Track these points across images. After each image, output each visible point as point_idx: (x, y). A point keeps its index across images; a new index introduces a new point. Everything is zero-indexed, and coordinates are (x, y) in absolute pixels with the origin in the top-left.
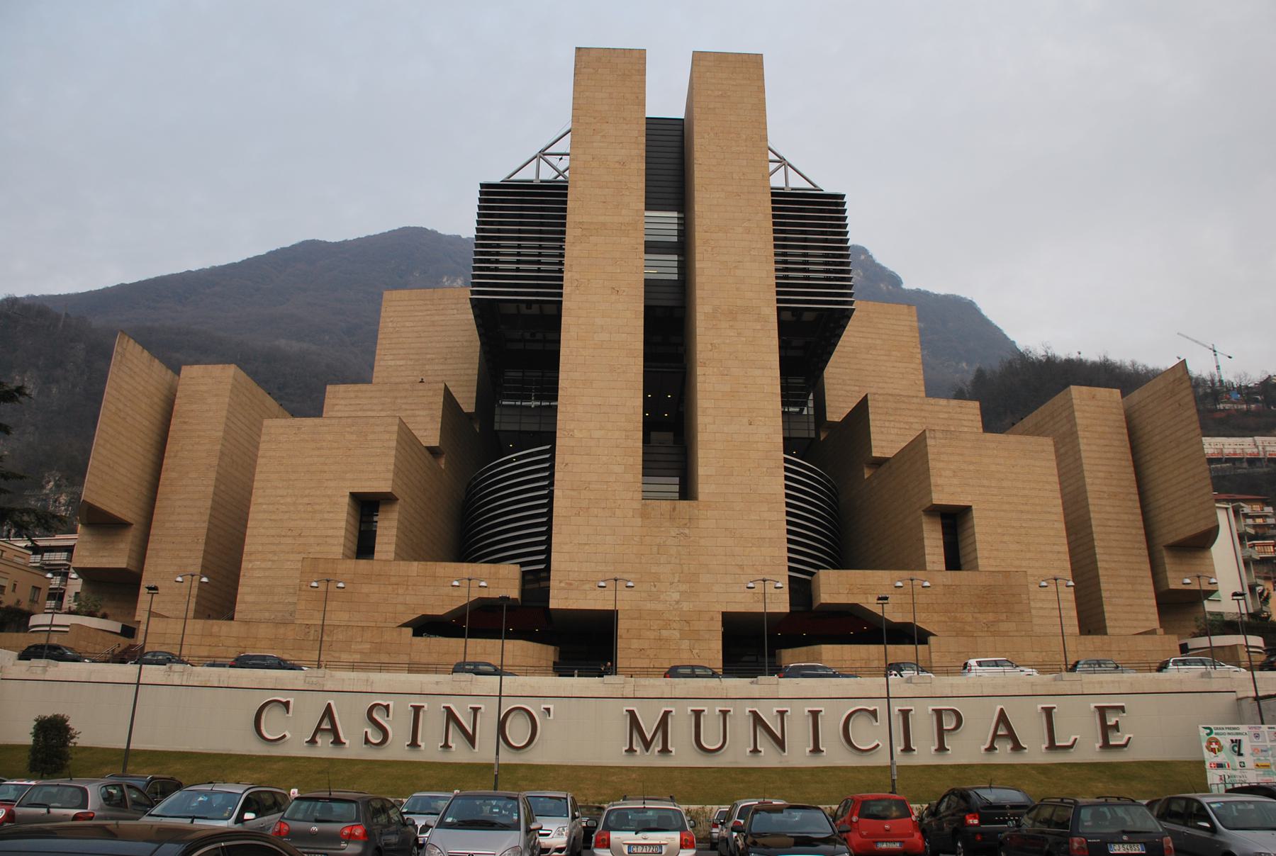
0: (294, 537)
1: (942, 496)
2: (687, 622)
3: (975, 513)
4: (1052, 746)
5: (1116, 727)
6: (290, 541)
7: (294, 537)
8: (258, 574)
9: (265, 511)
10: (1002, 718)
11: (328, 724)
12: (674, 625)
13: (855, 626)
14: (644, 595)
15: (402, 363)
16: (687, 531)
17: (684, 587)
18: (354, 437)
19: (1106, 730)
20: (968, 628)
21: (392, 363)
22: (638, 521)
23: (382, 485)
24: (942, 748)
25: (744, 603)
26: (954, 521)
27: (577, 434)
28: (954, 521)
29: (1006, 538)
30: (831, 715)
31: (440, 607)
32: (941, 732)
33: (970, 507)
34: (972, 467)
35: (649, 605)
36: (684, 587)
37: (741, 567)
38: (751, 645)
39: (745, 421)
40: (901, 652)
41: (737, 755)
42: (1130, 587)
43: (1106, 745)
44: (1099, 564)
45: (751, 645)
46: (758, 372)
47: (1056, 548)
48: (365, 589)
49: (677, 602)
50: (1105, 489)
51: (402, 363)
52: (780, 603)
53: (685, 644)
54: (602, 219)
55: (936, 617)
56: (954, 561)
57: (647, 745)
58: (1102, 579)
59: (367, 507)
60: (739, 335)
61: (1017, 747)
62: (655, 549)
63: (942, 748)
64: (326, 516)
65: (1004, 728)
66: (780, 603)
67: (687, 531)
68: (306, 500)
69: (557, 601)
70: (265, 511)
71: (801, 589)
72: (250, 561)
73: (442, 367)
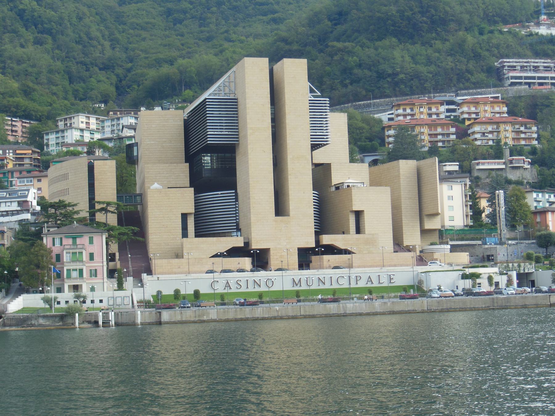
1: (355, 208)
3: (365, 212)
4: (379, 283)
10: (369, 277)
11: (228, 285)
13: (331, 250)
19: (391, 279)
21: (149, 142)
24: (357, 284)
26: (358, 214)
28: (358, 214)
30: (325, 274)
32: (357, 280)
40: (344, 258)
41: (315, 287)
56: (358, 231)
57: (297, 285)
58: (404, 227)
59: (184, 216)
61: (372, 283)
65: (370, 279)
71: (317, 241)
73: (170, 144)
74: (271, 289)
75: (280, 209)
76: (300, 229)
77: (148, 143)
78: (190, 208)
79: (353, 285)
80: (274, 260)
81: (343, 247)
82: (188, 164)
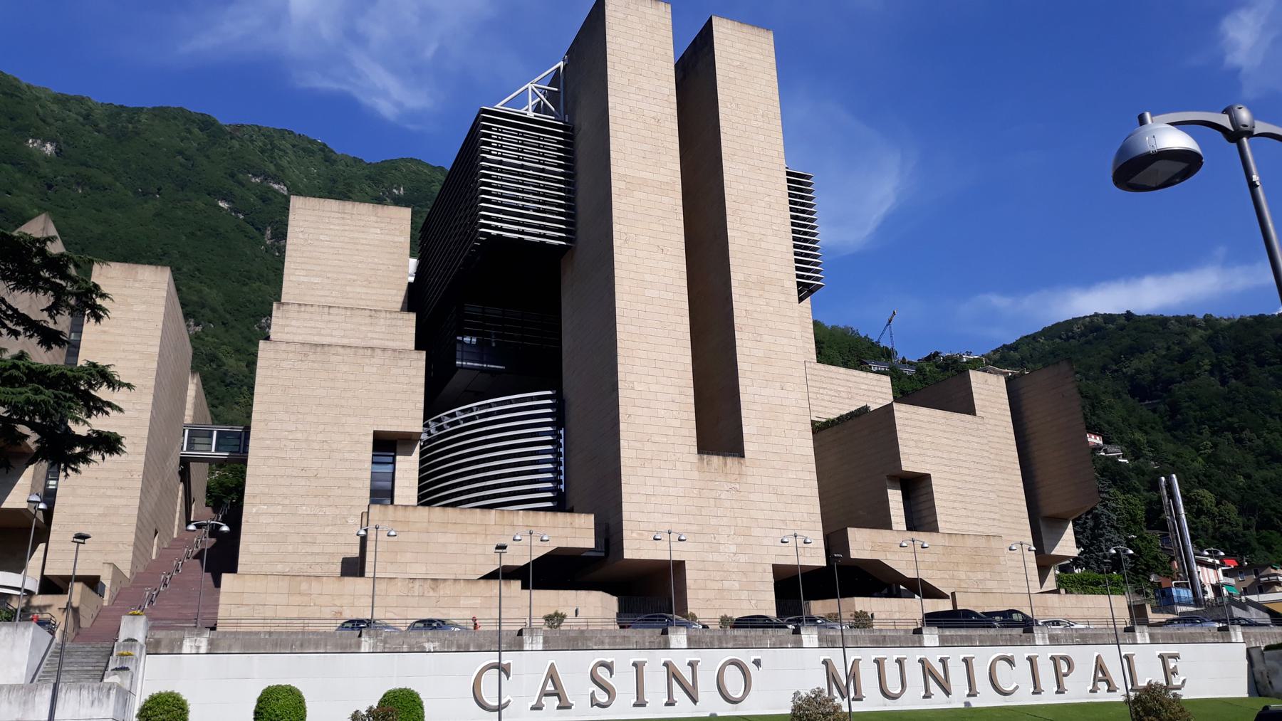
0: (308, 478)
1: (910, 464)
7: (308, 478)
8: (264, 520)
9: (268, 448)
12: (734, 576)
14: (706, 546)
15: (316, 280)
17: (740, 540)
18: (374, 370)
21: (306, 279)
22: (695, 475)
24: (1060, 690)
25: (788, 558)
27: (636, 386)
29: (956, 505)
31: (519, 557)
33: (927, 477)
34: (928, 439)
35: (710, 557)
36: (740, 540)
46: (785, 341)
48: (442, 538)
51: (316, 280)
52: (816, 558)
53: (744, 595)
54: (643, 174)
55: (939, 574)
59: (387, 445)
60: (767, 304)
63: (1060, 690)
64: (347, 455)
66: (816, 558)
68: (321, 437)
70: (268, 448)
72: (253, 505)
73: (364, 290)
74: (742, 710)
75: (719, 429)
77: (302, 279)
78: (408, 415)
79: (1049, 697)
80: (704, 599)
82: (413, 316)
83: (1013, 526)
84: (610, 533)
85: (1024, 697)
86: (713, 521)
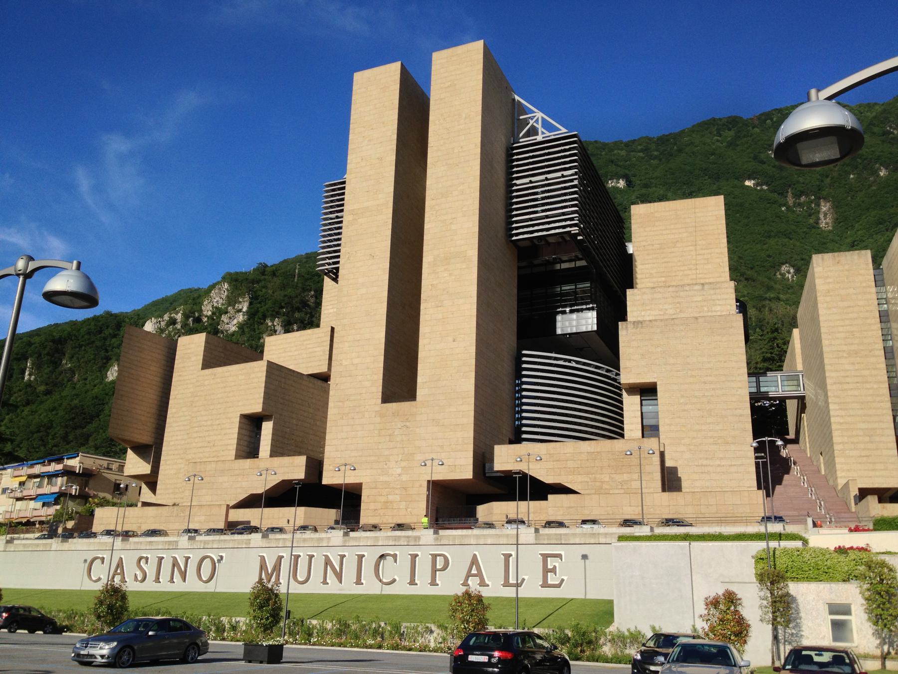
2: (405, 489)
5: (554, 570)
6: (208, 449)
12: (397, 492)
16: (408, 424)
17: (404, 464)
19: (546, 571)
20: (605, 486)
22: (378, 420)
23: (256, 406)
24: (433, 583)
25: (442, 474)
27: (345, 363)
31: (260, 487)
32: (434, 570)
34: (659, 349)
35: (382, 478)
36: (404, 464)
37: (442, 447)
38: (453, 504)
39: (451, 339)
42: (867, 439)
43: (545, 585)
44: (833, 420)
45: (453, 504)
47: (739, 412)
49: (399, 475)
50: (845, 348)
52: (466, 473)
55: (580, 478)
62: (388, 438)
63: (433, 583)
64: (228, 431)
66: (466, 473)
67: (408, 424)
68: (218, 422)
69: (328, 479)
76: (441, 433)
79: (423, 588)
81: (548, 479)
83: (860, 412)
84: (315, 466)
85: (402, 588)
86: (386, 453)
